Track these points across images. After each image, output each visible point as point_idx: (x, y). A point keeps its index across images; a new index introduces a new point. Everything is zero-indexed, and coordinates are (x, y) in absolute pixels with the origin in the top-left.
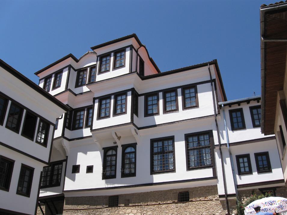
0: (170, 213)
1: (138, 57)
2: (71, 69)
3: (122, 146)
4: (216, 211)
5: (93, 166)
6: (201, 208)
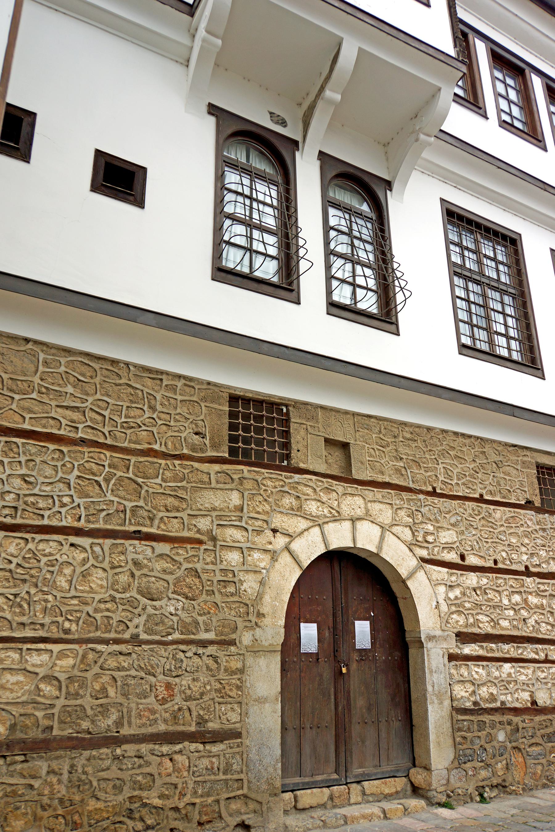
0: (524, 549)
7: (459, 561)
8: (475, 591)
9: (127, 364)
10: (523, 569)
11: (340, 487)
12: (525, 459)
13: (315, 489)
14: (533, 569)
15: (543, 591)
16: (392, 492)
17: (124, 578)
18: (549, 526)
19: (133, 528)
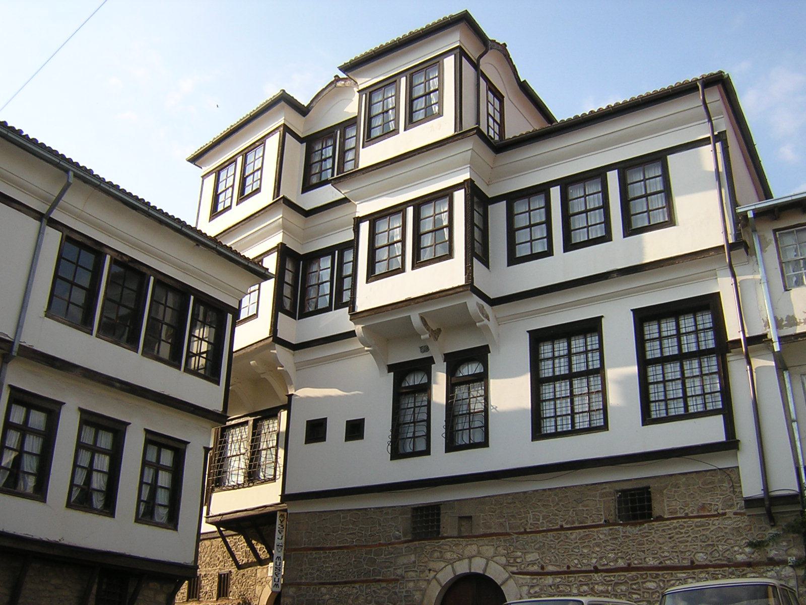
0: (594, 555)
1: (483, 83)
2: (287, 134)
3: (448, 357)
4: (736, 548)
5: (363, 419)
6: (690, 539)
7: (540, 570)
8: (551, 587)
9: (370, 508)
10: (592, 569)
11: (463, 542)
12: (604, 491)
13: (450, 547)
14: (600, 568)
15: (609, 581)
16: (494, 537)
17: (369, 598)
18: (622, 534)
19: (372, 578)
